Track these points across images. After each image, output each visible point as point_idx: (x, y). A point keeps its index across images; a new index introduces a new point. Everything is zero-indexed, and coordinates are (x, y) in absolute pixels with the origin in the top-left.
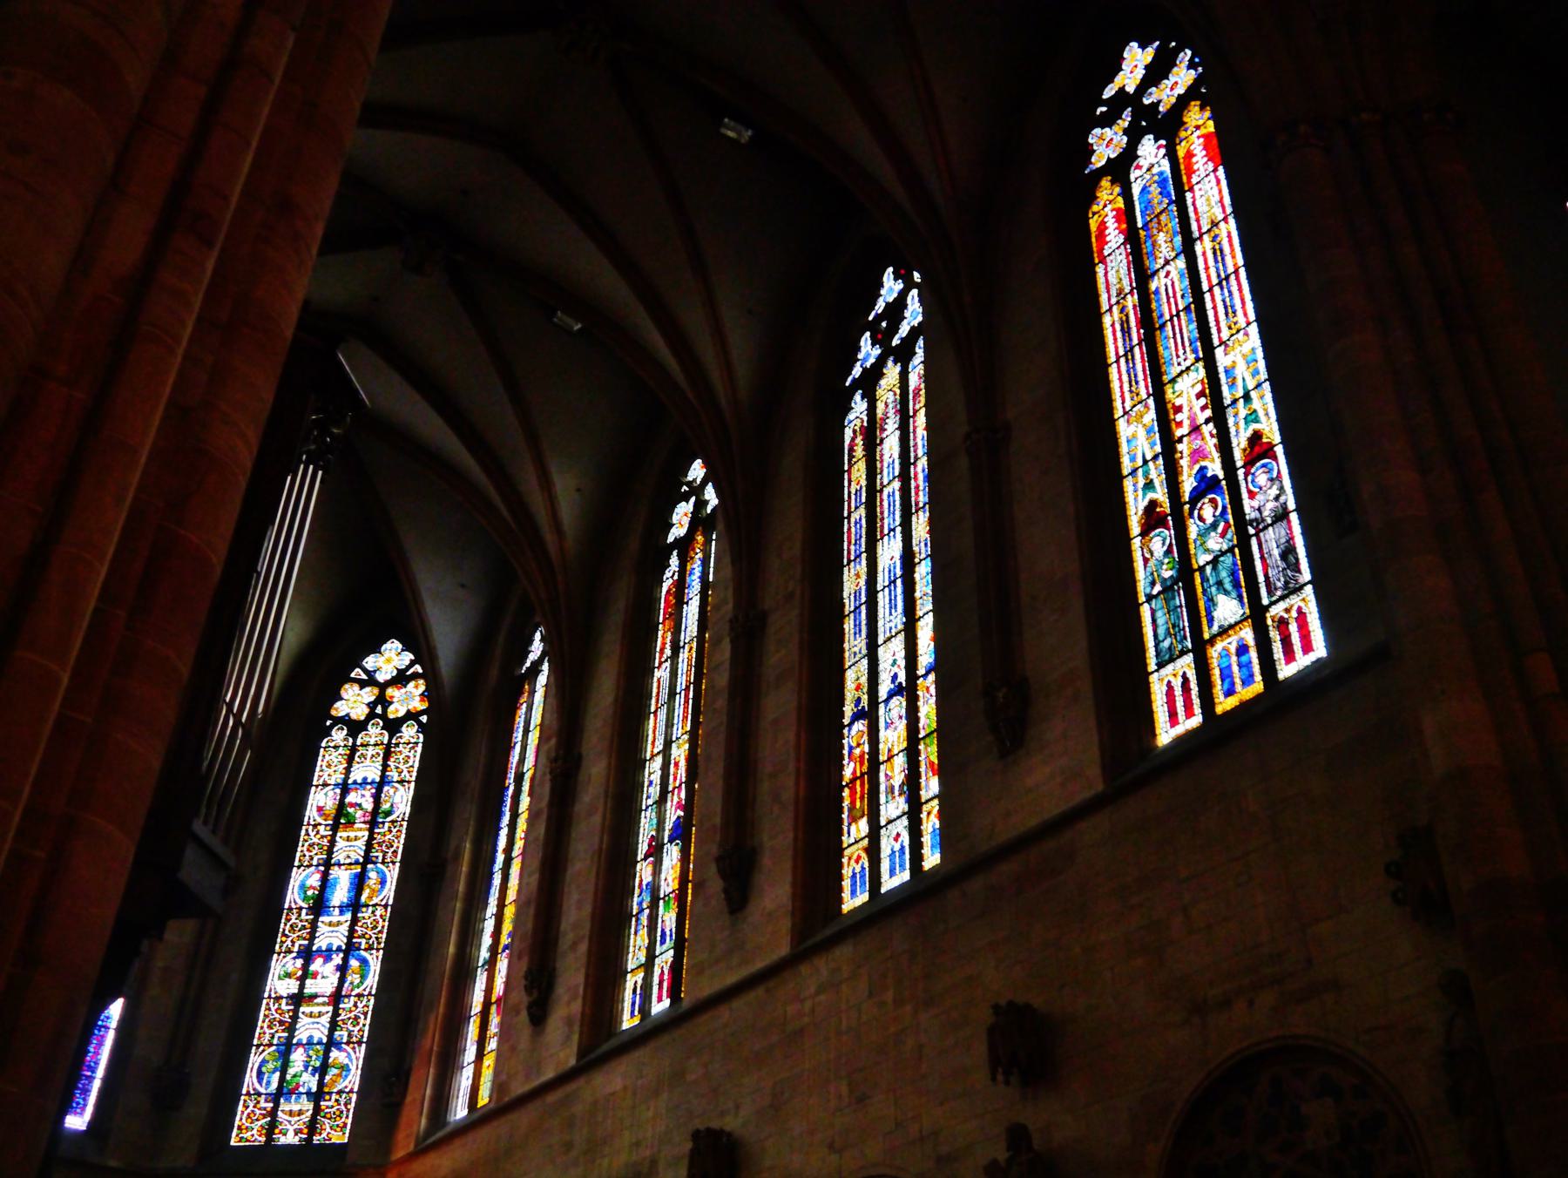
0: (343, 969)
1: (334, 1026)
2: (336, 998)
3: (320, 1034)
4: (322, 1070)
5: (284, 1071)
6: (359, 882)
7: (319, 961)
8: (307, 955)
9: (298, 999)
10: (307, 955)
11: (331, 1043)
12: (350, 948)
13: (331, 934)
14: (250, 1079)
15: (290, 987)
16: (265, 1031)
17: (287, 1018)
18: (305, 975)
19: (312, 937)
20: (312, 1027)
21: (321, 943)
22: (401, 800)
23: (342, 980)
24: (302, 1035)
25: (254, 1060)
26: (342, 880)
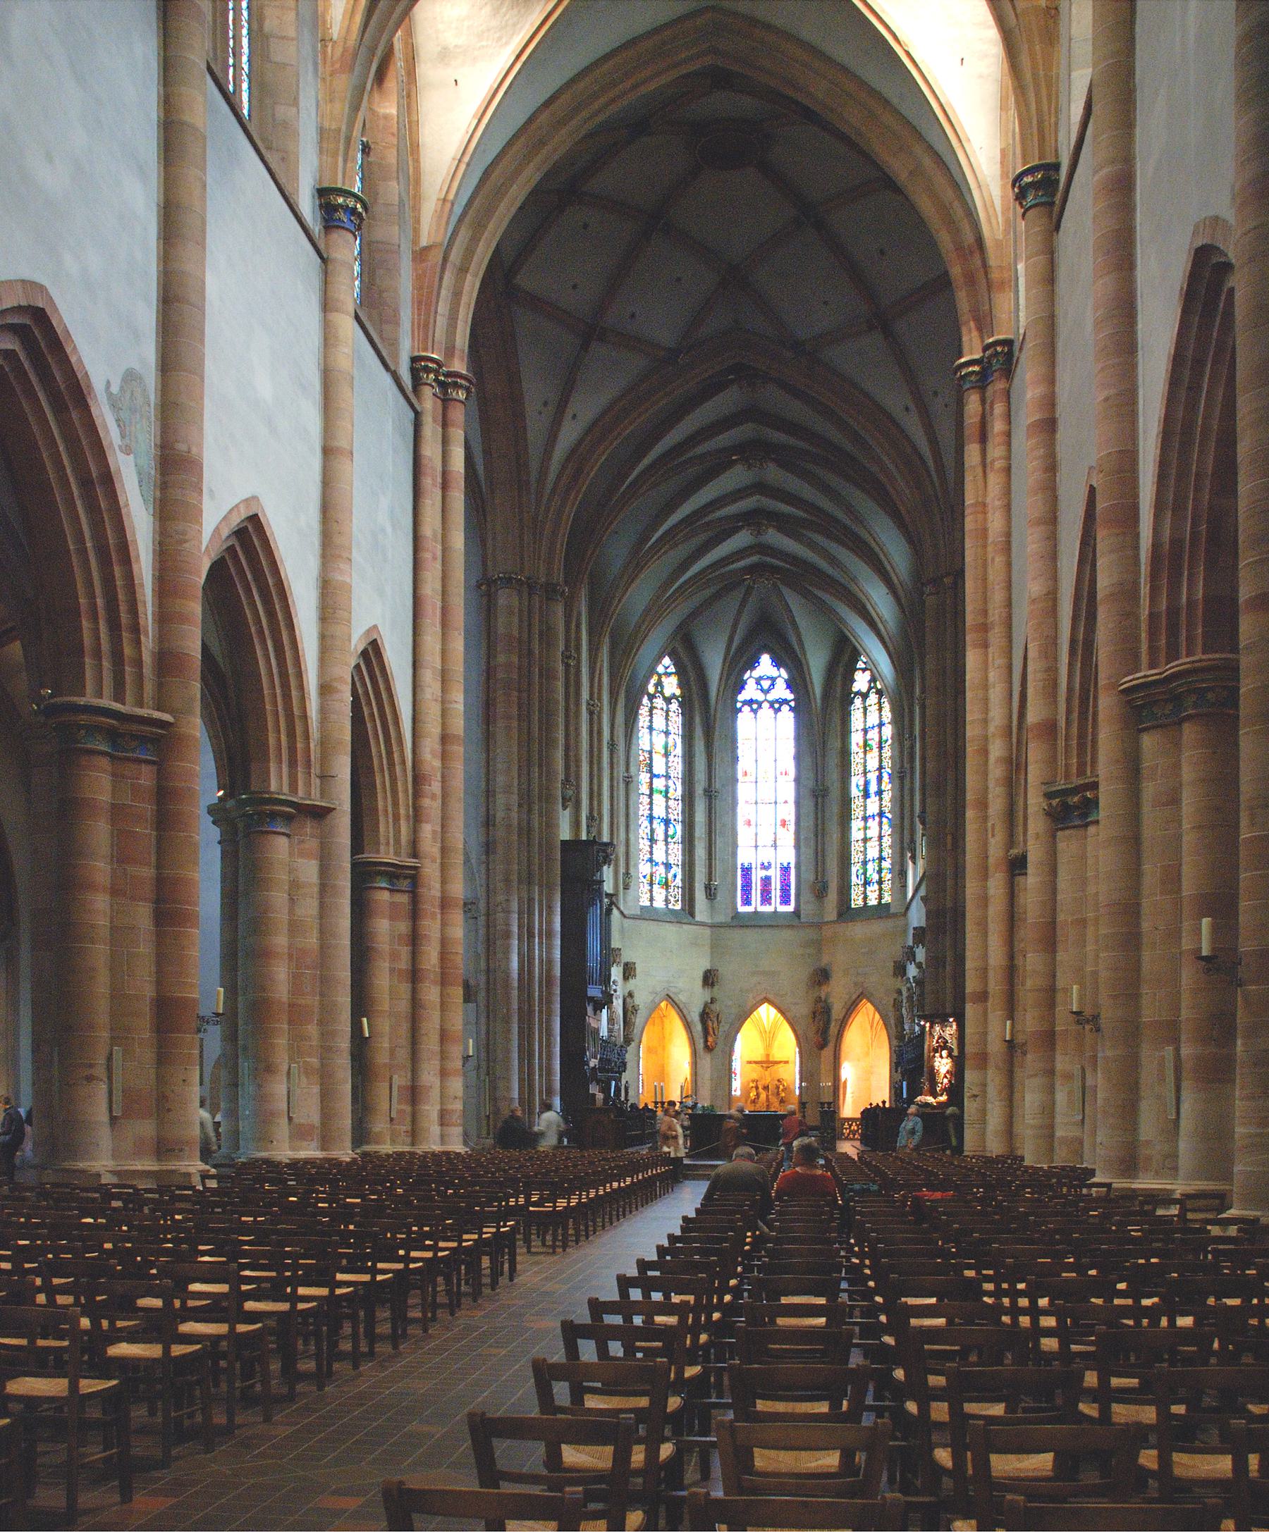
0: (880, 823)
1: (881, 851)
2: (880, 838)
3: (877, 856)
4: (880, 872)
5: (865, 873)
6: (880, 779)
7: (870, 820)
8: (865, 819)
9: (865, 840)
10: (865, 819)
11: (881, 859)
12: (881, 814)
13: (873, 807)
14: (854, 878)
15: (860, 835)
16: (856, 857)
17: (862, 849)
18: (865, 828)
19: (865, 809)
20: (873, 853)
21: (869, 813)
22: (888, 731)
23: (881, 828)
24: (869, 857)
25: (854, 869)
26: (872, 777)
